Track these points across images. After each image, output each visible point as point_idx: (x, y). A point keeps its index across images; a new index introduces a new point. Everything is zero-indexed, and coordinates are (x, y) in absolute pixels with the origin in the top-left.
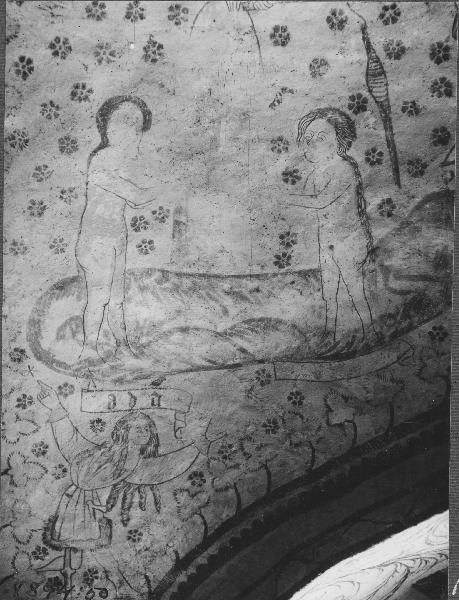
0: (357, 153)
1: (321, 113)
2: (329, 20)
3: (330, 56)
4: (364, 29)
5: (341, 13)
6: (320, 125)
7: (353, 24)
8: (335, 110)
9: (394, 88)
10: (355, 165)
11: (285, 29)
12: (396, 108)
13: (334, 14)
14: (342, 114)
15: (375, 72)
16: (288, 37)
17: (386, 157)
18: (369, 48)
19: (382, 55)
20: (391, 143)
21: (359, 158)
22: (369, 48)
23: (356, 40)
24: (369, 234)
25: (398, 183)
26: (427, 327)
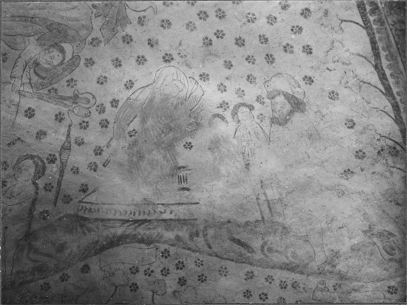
0: (41, 183)
1: (32, 157)
2: (56, 115)
3: (49, 132)
4: (70, 126)
5: (63, 115)
6: (30, 162)
7: (67, 122)
8: (39, 158)
9: (72, 158)
10: (37, 188)
11: (33, 111)
12: (68, 169)
13: (60, 114)
14: (42, 161)
15: (66, 148)
16: (33, 115)
17: (54, 190)
18: (68, 135)
19: (73, 141)
20: (59, 183)
21: (41, 186)
22: (68, 135)
23: (63, 130)
24: (30, 225)
25: (55, 204)
26: (41, 282)
